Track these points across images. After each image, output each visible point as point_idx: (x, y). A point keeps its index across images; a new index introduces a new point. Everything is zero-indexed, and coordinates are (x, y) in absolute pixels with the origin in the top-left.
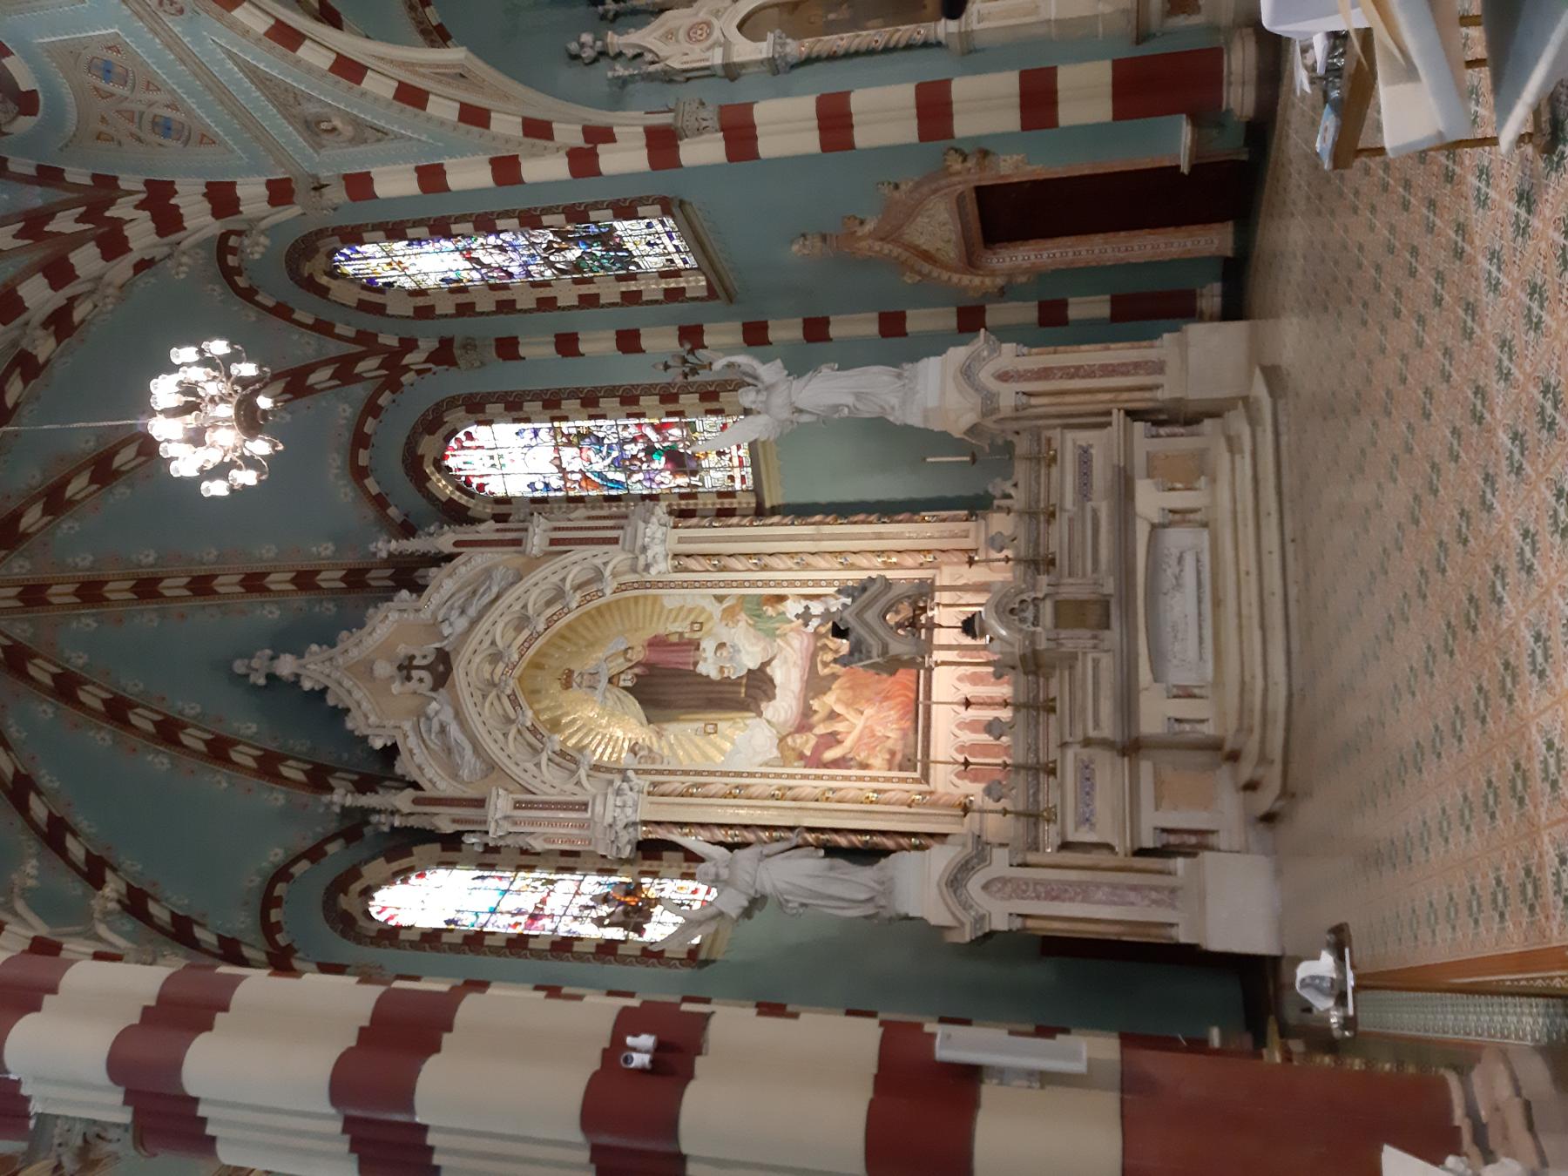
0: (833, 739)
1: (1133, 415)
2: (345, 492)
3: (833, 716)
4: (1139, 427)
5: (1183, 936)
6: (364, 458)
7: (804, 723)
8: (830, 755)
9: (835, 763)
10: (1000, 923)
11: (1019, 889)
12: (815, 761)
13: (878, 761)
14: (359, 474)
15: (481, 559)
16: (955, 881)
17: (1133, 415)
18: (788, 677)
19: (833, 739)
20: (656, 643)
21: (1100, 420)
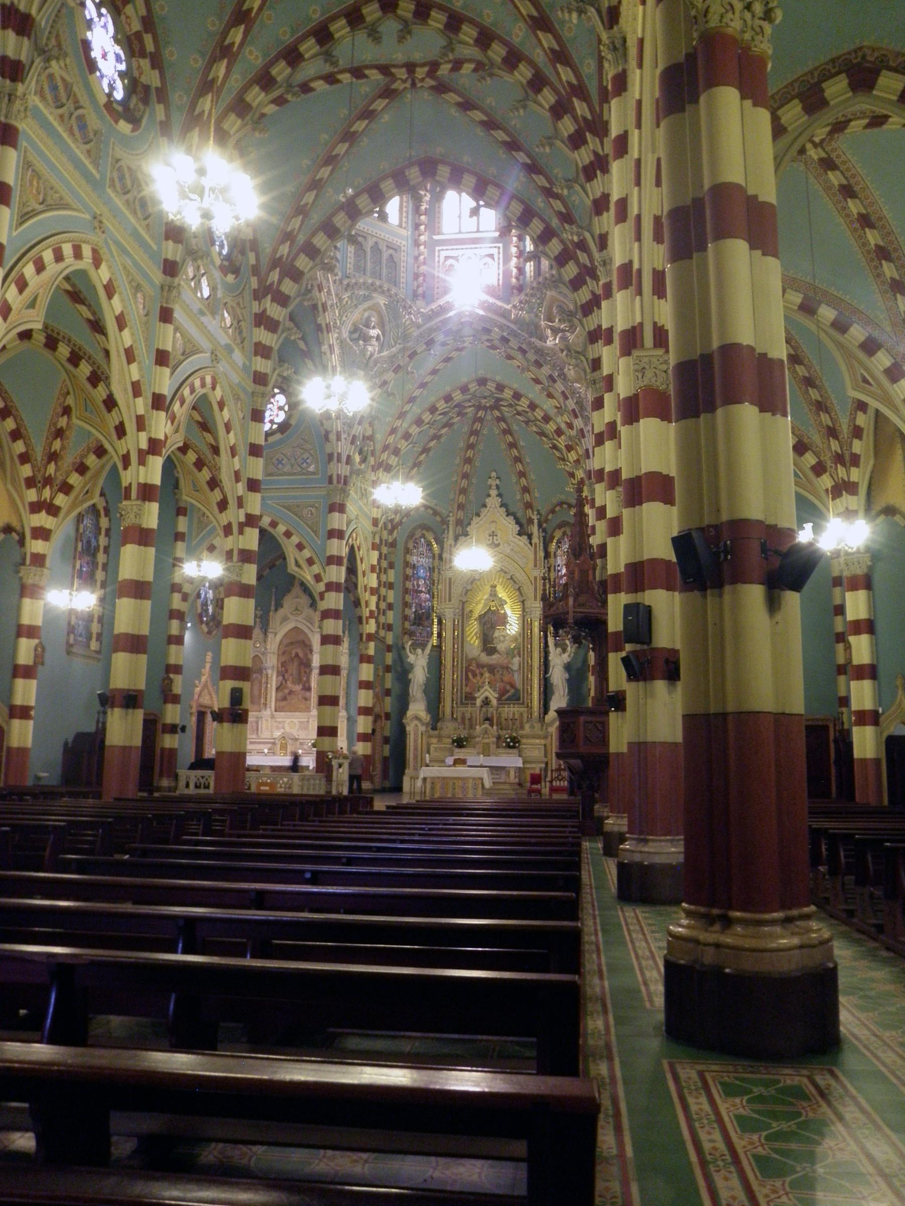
0: (474, 675)
1: (547, 764)
2: (555, 501)
3: (482, 675)
4: (543, 765)
5: (407, 771)
6: (565, 506)
7: (480, 666)
8: (470, 675)
9: (467, 679)
10: (408, 729)
11: (416, 734)
12: (468, 670)
13: (468, 689)
14: (561, 504)
15: (531, 556)
16: (417, 718)
17: (547, 764)
18: (494, 659)
19: (474, 675)
20: (505, 616)
21: (546, 756)
